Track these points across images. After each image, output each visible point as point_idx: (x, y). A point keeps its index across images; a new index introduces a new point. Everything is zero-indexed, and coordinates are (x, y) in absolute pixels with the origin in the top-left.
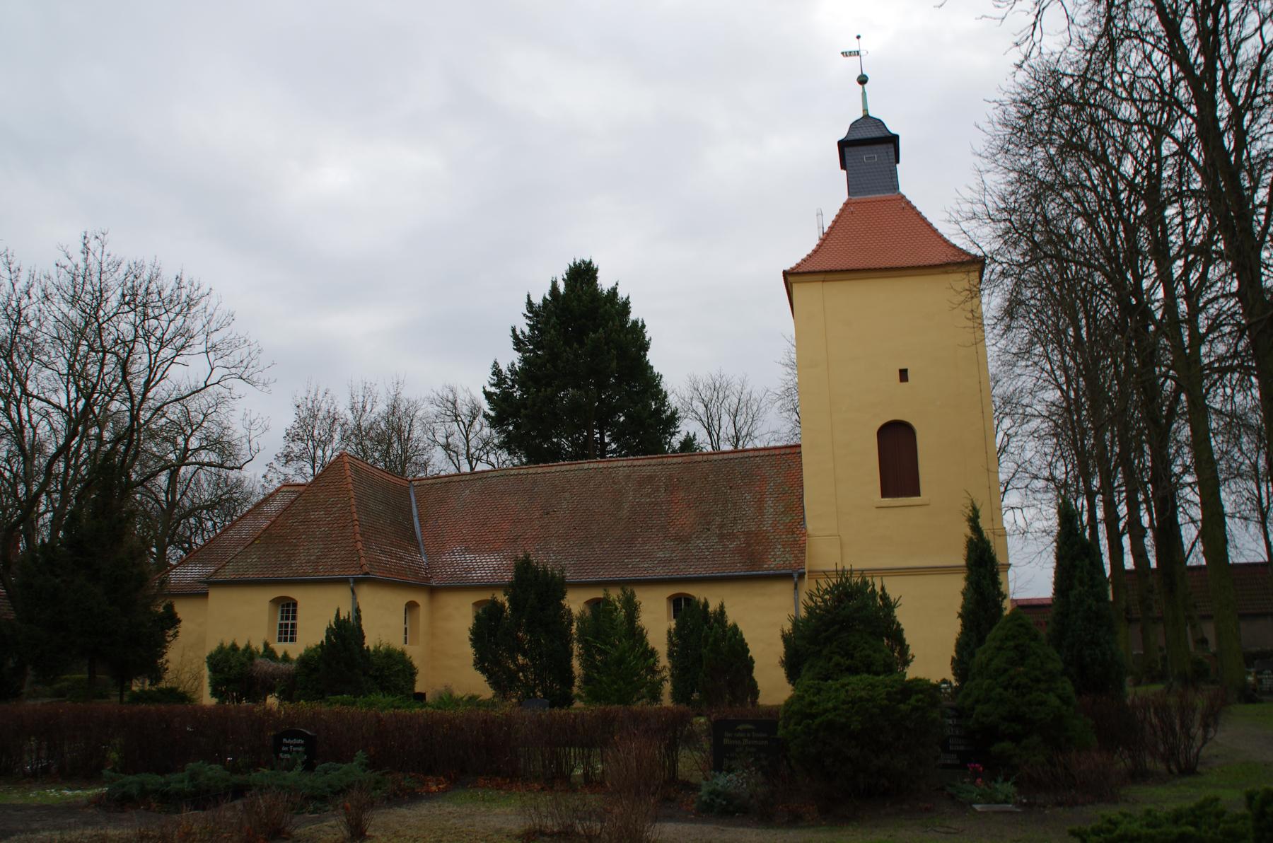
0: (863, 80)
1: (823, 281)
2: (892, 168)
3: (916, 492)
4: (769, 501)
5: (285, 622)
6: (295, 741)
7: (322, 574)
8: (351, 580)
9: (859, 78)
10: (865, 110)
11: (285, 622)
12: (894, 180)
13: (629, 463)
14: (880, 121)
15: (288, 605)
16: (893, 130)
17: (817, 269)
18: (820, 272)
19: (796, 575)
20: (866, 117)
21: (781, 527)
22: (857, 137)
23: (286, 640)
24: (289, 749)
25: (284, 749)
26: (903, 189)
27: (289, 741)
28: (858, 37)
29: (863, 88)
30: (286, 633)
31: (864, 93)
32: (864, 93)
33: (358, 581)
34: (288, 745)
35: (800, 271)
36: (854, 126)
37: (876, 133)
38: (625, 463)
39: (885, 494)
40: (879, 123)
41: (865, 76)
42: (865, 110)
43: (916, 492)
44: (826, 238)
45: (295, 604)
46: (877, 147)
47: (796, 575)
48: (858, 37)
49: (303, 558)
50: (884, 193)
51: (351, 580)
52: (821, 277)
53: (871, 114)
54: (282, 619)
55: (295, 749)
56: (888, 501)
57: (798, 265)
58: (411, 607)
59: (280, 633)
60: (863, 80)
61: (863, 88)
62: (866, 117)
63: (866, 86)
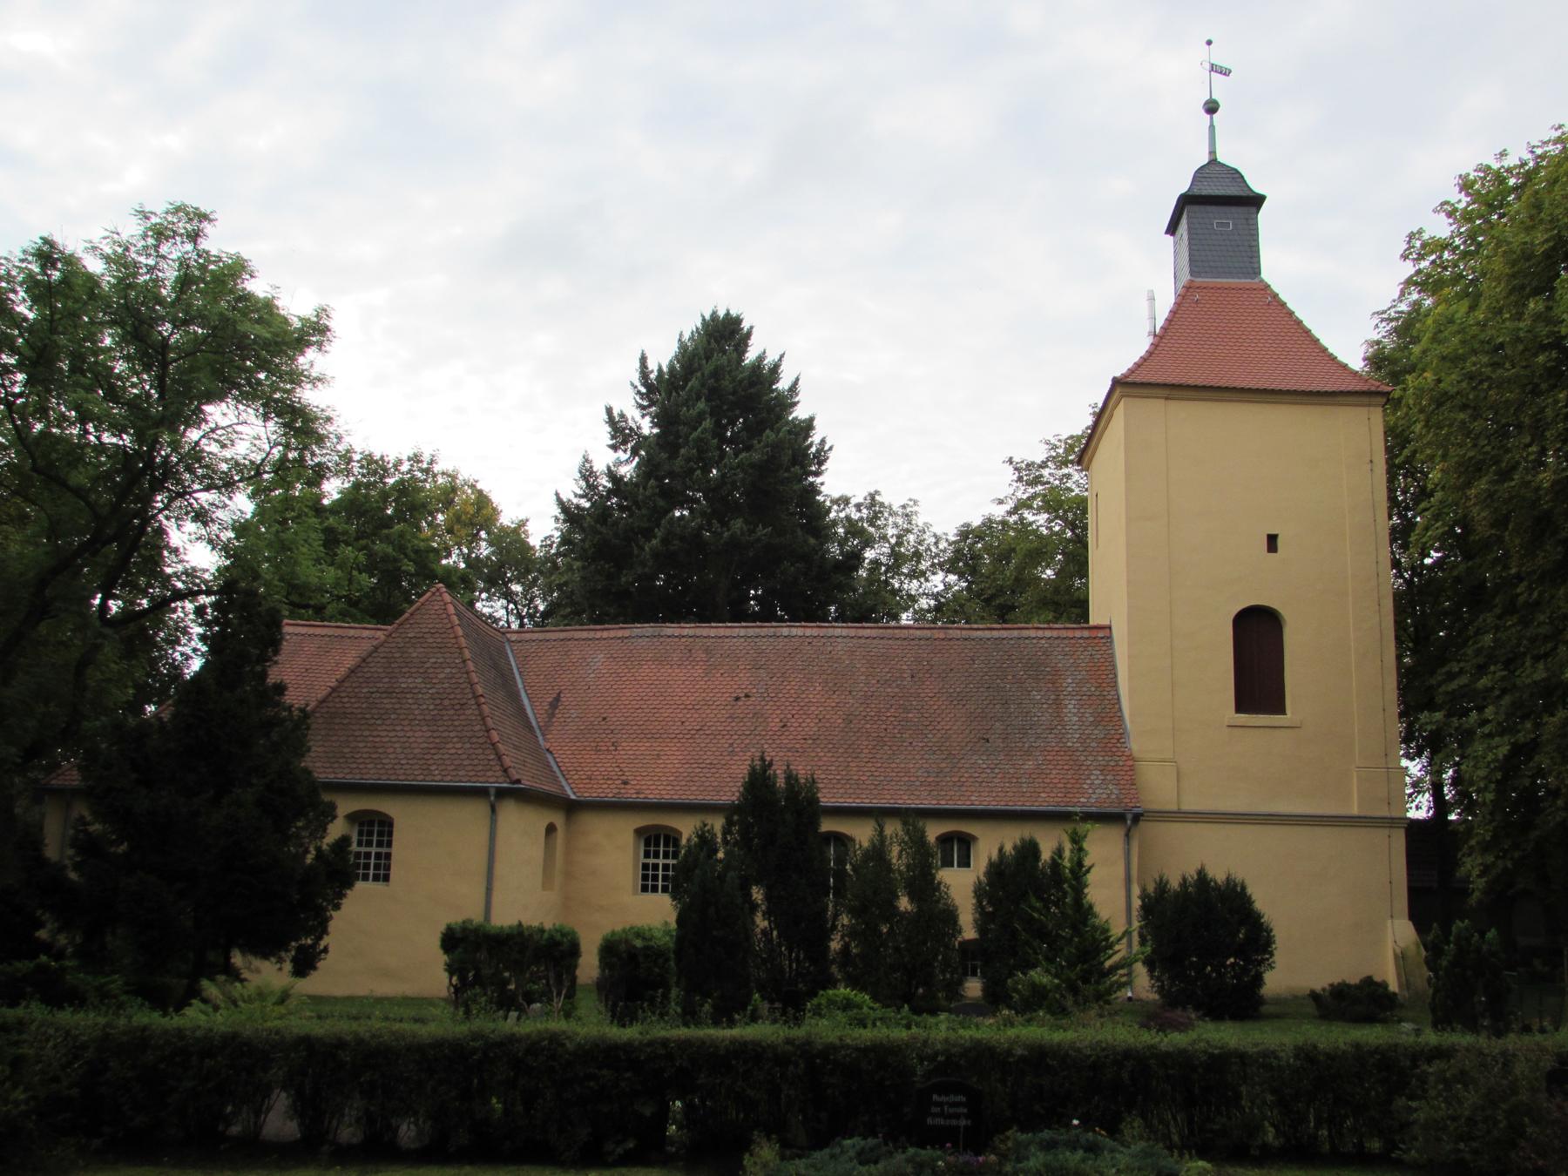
0: (1211, 108)
1: (1167, 398)
2: (1253, 243)
3: (1282, 711)
4: (1071, 706)
5: (651, 861)
6: (953, 1098)
7: (439, 778)
8: (492, 792)
9: (1206, 103)
10: (1212, 152)
11: (651, 861)
12: (1255, 260)
13: (1055, 634)
14: (1237, 172)
15: (371, 823)
16: (1257, 187)
17: (1160, 380)
18: (1165, 386)
19: (1129, 816)
20: (1213, 162)
21: (1094, 744)
22: (1204, 193)
23: (655, 889)
24: (943, 1110)
25: (935, 1110)
26: (1266, 275)
27: (943, 1099)
28: (1209, 43)
29: (1212, 119)
30: (377, 867)
31: (1212, 127)
32: (1212, 127)
33: (502, 794)
34: (940, 1104)
35: (1138, 380)
36: (1200, 174)
37: (1232, 191)
38: (1048, 634)
39: (1241, 707)
40: (1236, 175)
41: (1215, 102)
42: (1212, 152)
43: (1282, 711)
44: (1161, 339)
45: (391, 825)
46: (1234, 209)
47: (1129, 816)
48: (1209, 43)
49: (399, 750)
50: (1239, 278)
51: (492, 792)
52: (1166, 392)
53: (1220, 159)
54: (647, 855)
55: (951, 1110)
56: (1244, 718)
57: (1132, 371)
58: (551, 829)
59: (388, 868)
60: (1211, 108)
61: (1212, 119)
62: (1213, 162)
63: (1214, 116)
